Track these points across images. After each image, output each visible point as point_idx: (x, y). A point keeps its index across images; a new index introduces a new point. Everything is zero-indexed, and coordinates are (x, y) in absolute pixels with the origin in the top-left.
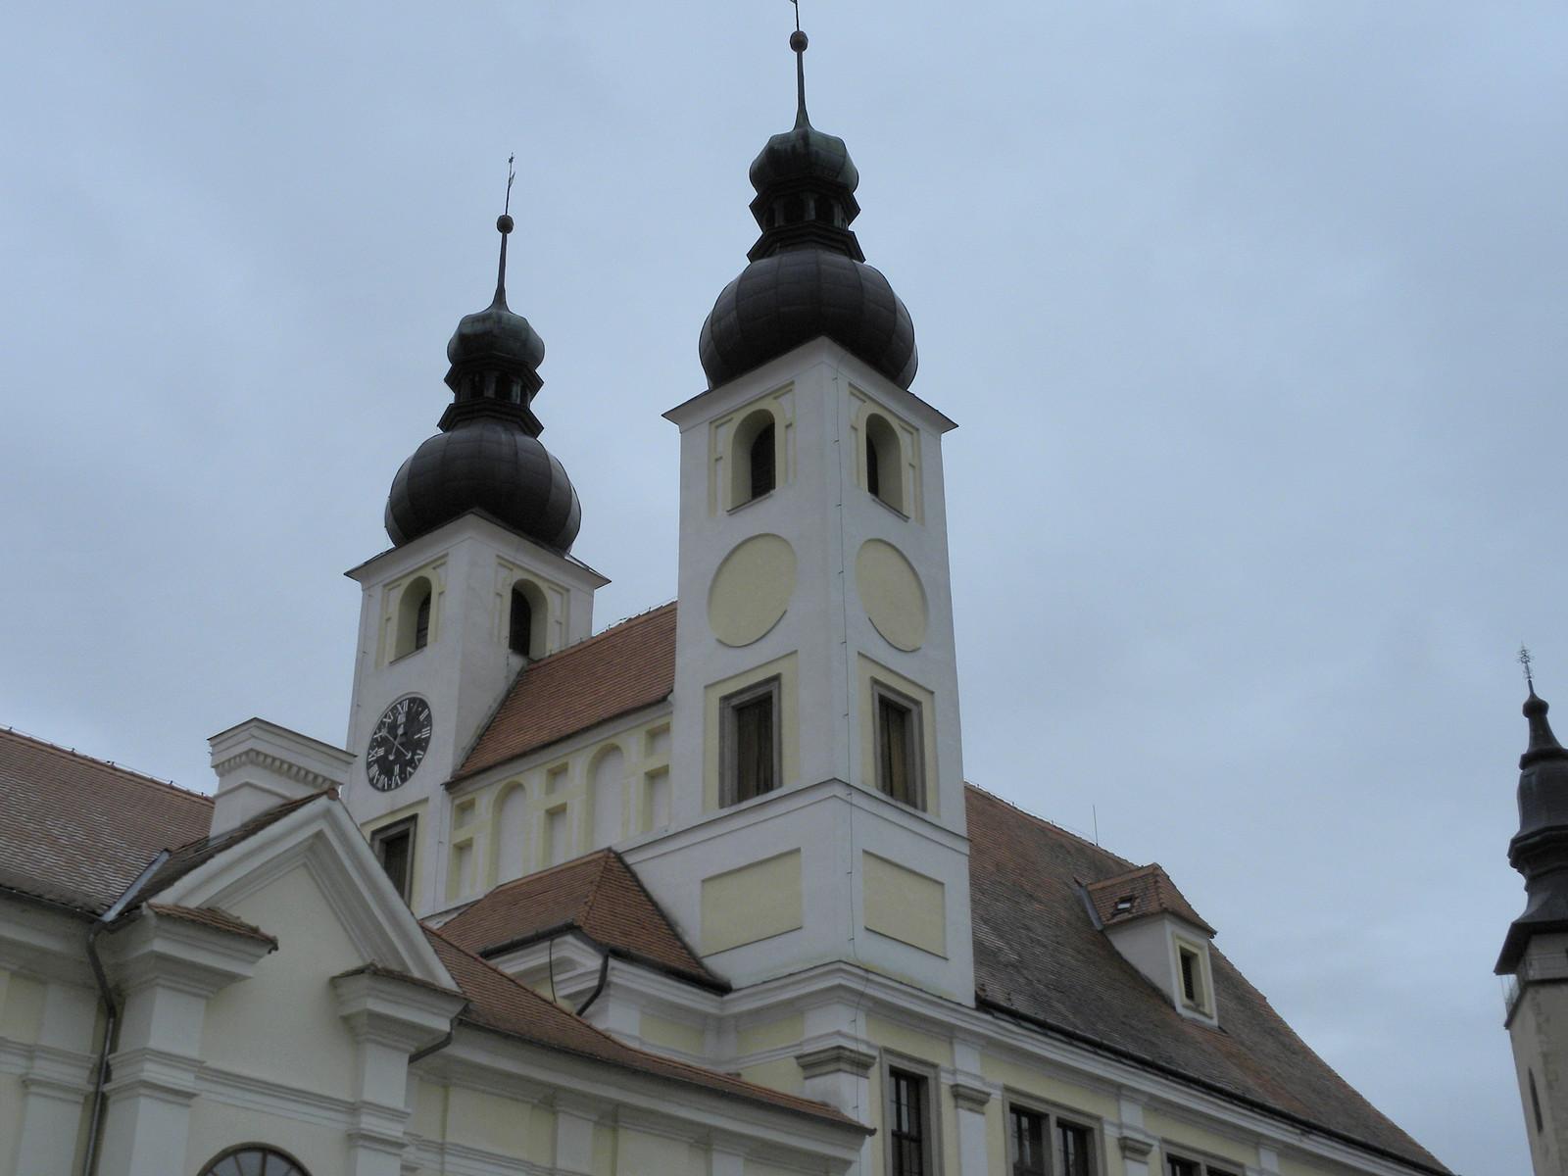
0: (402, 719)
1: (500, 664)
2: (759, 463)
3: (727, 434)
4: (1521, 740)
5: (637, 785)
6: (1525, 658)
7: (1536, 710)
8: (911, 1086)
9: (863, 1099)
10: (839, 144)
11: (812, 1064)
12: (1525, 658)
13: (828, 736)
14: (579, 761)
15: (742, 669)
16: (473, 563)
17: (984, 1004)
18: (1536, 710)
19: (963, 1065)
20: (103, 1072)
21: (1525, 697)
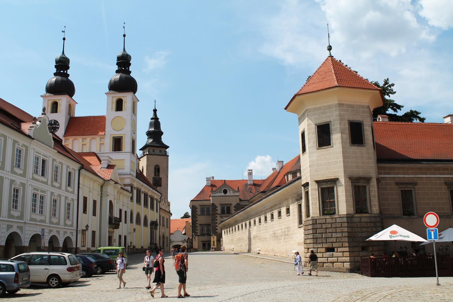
0: (53, 123)
1: (68, 117)
2: (119, 106)
3: (115, 100)
4: (152, 115)
5: (98, 145)
6: (155, 102)
7: (155, 111)
8: (132, 187)
9: (129, 188)
10: (130, 56)
11: (125, 185)
12: (155, 102)
13: (126, 145)
14: (88, 138)
15: (117, 134)
16: (63, 100)
17: (137, 177)
18: (155, 111)
19: (135, 185)
20: (101, 194)
21: (154, 108)
